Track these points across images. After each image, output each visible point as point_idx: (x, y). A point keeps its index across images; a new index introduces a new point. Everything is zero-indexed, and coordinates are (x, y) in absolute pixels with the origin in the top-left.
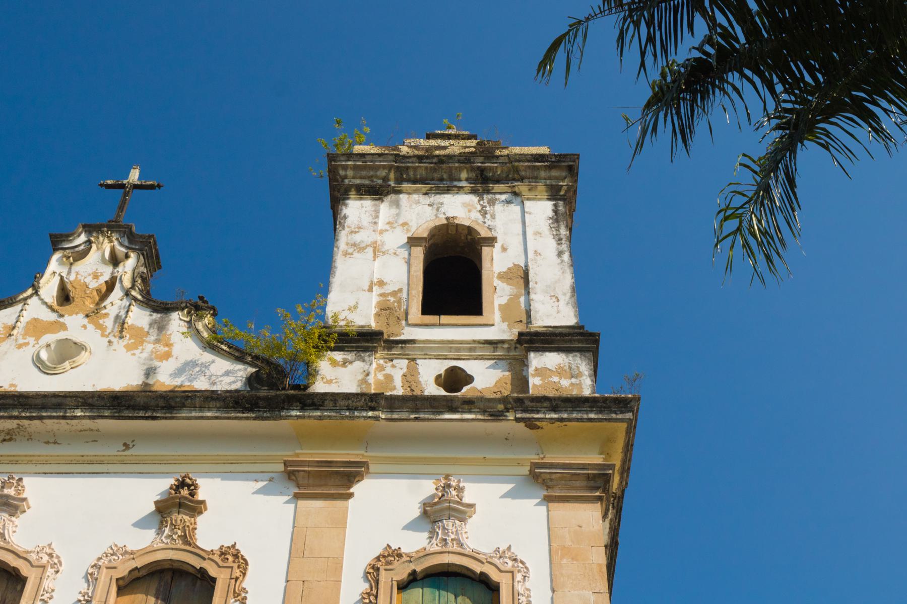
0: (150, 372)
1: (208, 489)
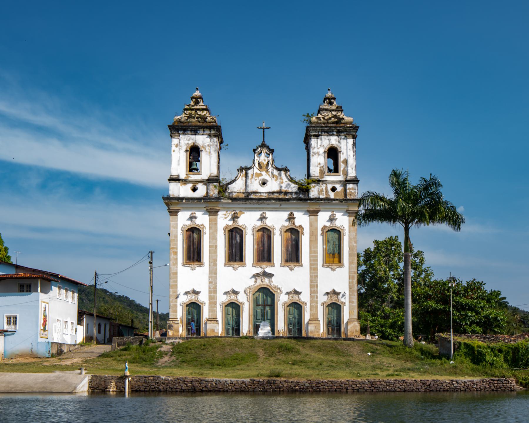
1: (296, 214)
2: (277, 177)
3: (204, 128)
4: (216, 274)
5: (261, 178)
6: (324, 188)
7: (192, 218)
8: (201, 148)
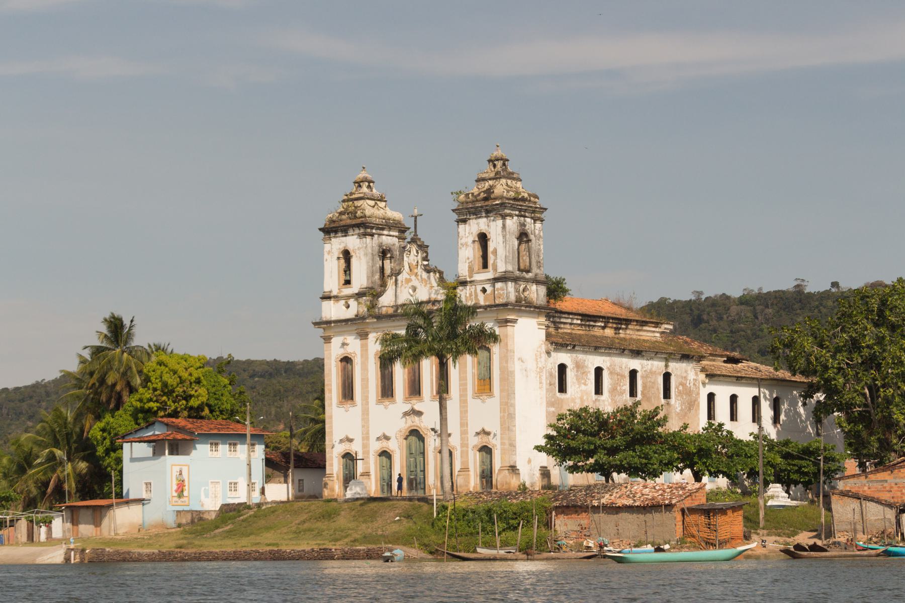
0: (430, 294)
2: (426, 282)
3: (354, 226)
4: (368, 414)
5: (410, 284)
6: (473, 290)
7: (344, 344)
8: (352, 253)
